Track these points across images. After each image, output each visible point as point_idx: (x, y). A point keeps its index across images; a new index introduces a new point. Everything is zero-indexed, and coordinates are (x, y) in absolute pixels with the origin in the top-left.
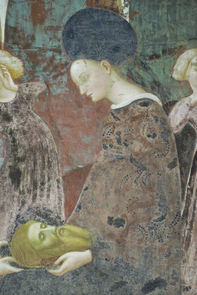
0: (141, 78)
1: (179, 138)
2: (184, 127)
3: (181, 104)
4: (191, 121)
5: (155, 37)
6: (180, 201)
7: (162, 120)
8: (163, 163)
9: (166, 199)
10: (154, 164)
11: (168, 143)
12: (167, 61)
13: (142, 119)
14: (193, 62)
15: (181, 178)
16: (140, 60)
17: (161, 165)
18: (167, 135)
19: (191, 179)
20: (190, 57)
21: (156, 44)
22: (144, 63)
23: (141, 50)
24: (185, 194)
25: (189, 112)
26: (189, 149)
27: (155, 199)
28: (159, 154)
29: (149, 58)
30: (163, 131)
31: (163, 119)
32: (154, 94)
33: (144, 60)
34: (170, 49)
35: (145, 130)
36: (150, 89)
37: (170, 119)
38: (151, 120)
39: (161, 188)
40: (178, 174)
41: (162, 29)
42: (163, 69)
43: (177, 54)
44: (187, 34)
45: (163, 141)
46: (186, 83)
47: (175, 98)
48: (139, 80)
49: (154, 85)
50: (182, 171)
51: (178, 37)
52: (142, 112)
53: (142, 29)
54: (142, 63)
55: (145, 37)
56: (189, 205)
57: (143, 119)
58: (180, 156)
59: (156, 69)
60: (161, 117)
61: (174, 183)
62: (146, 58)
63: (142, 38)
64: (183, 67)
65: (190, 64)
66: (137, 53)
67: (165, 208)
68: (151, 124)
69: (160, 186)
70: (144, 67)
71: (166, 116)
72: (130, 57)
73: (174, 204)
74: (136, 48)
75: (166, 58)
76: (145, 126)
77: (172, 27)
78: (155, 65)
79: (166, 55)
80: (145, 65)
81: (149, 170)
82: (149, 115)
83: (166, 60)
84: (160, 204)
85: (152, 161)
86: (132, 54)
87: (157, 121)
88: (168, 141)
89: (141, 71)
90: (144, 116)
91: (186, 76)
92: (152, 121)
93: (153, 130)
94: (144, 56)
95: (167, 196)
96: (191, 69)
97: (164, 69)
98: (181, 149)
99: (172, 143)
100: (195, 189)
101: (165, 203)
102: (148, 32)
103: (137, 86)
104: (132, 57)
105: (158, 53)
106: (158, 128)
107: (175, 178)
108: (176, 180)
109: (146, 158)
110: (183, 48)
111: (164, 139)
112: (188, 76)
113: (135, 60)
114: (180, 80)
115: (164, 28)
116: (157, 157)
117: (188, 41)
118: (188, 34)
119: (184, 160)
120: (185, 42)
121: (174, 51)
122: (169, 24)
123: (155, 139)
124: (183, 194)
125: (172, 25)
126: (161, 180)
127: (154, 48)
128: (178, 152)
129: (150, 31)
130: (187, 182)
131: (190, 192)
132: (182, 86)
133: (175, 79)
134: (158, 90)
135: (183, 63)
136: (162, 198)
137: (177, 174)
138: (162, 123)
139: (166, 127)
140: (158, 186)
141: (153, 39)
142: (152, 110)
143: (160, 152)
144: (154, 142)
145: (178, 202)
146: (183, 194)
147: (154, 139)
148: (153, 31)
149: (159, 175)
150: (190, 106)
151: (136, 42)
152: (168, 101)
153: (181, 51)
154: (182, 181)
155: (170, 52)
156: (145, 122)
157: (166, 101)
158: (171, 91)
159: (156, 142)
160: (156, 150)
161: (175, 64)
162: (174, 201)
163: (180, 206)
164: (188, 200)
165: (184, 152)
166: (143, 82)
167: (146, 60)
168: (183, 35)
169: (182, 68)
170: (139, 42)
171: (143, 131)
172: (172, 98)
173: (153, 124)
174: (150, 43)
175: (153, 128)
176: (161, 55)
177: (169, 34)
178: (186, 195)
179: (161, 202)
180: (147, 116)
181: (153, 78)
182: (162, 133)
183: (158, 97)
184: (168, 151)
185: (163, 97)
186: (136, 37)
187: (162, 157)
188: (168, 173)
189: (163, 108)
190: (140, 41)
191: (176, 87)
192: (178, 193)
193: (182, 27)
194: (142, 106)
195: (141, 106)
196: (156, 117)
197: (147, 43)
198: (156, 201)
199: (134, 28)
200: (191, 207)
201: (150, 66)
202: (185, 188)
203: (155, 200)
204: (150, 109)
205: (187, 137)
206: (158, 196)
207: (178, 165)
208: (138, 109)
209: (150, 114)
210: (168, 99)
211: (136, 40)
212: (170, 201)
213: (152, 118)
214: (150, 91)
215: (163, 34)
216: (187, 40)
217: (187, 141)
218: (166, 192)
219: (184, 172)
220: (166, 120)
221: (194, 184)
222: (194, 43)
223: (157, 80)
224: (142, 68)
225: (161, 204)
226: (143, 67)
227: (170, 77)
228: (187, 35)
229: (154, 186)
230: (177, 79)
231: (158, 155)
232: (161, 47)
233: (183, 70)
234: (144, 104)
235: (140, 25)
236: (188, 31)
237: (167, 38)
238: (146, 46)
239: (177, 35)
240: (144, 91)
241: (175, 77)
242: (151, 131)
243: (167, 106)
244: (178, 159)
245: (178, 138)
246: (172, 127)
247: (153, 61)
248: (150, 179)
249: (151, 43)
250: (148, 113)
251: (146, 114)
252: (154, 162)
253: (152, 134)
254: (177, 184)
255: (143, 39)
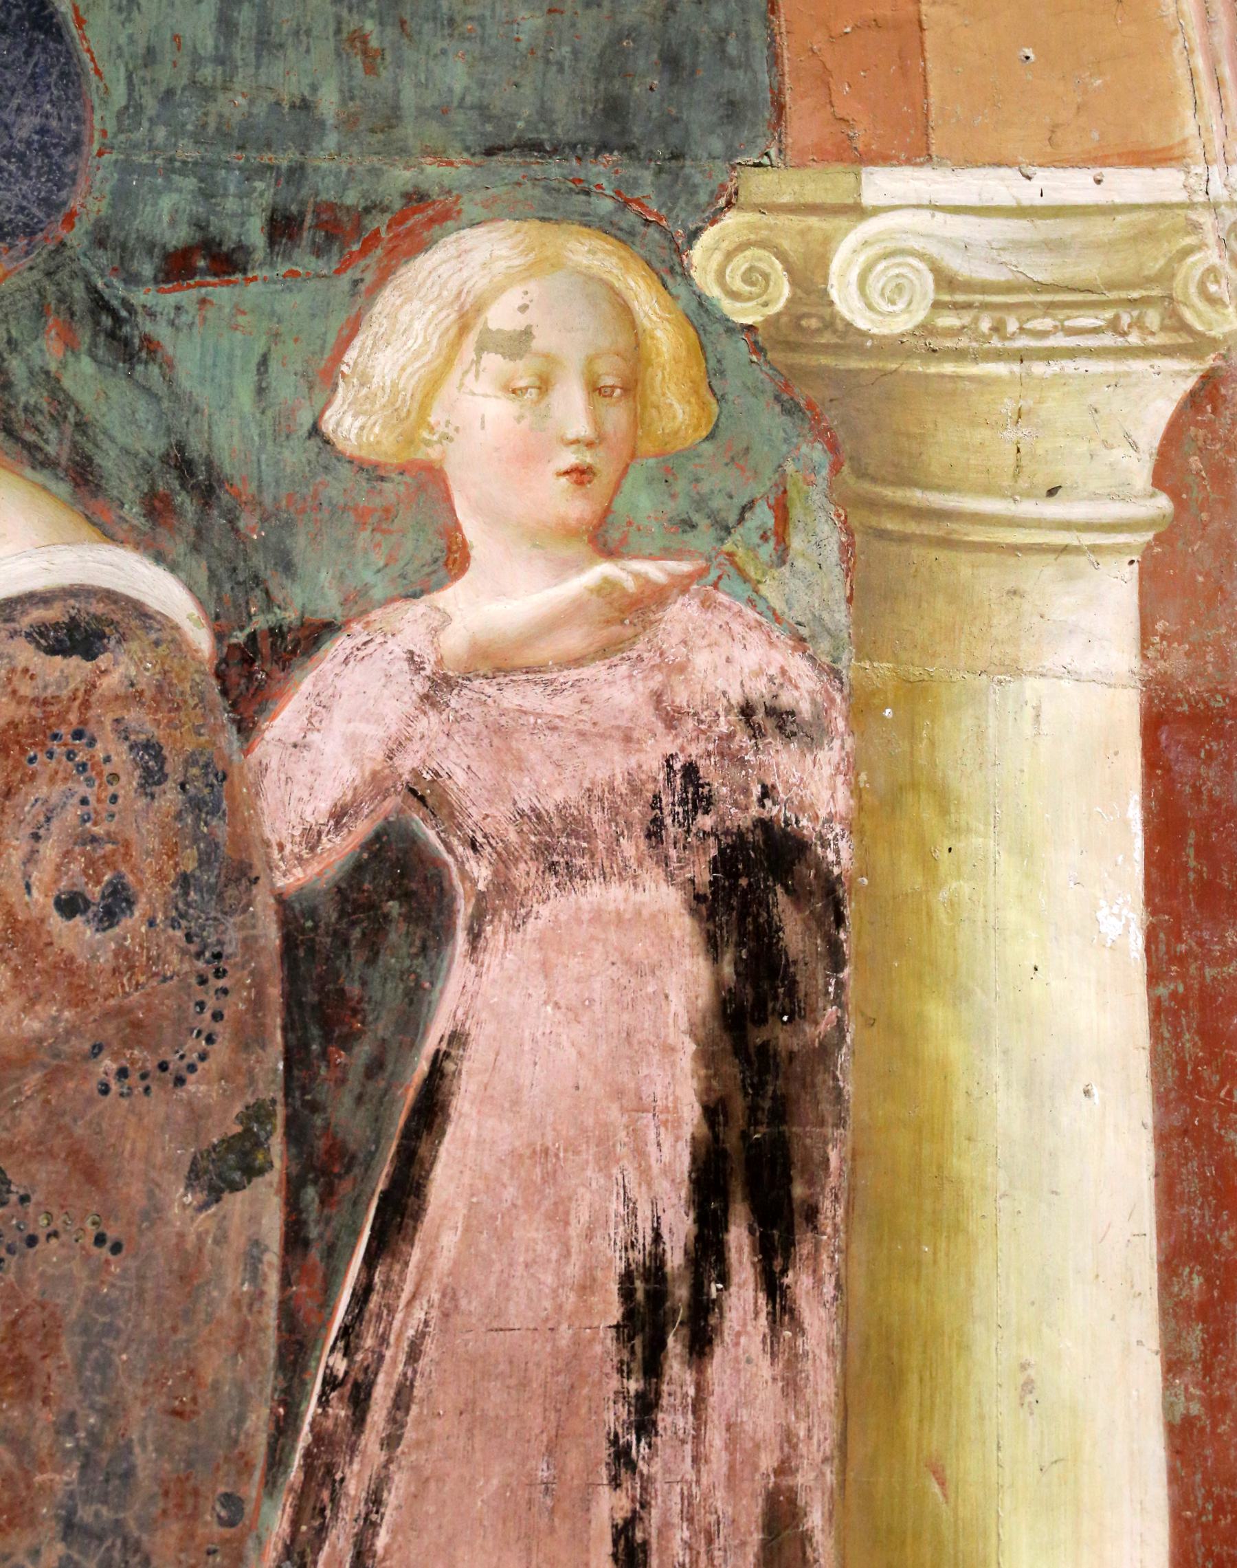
0: (77, 425)
1: (315, 928)
2: (366, 846)
3: (361, 654)
4: (422, 799)
5: (227, 111)
6: (252, 1489)
7: (195, 771)
8: (150, 1148)
9: (128, 1475)
10: (74, 1153)
11: (220, 974)
12: (294, 302)
13: (31, 760)
14: (493, 326)
15: (286, 1282)
16: (86, 277)
17: (132, 1155)
18: (221, 898)
19: (362, 1295)
20: (480, 282)
21: (228, 166)
22: (115, 303)
23: (109, 197)
24: (297, 1431)
25: (422, 725)
26: (382, 1027)
27: (42, 1467)
28: (133, 1062)
29: (158, 270)
30: (190, 866)
31: (207, 766)
32: (159, 558)
33: (116, 282)
34: (331, 207)
35: (50, 851)
36: (133, 512)
37: (263, 769)
38: (108, 769)
39: (104, 1365)
40: (266, 1249)
41: (291, 53)
42: (256, 359)
43: (379, 252)
44: (472, 108)
45: (184, 952)
46: (421, 487)
47: (323, 596)
48: (53, 435)
49: (168, 482)
50: (305, 1223)
51: (399, 118)
52: (45, 703)
53: (131, 39)
54: (99, 304)
55: (151, 105)
56: (321, 1533)
57: (42, 757)
58: (304, 1090)
59: (203, 355)
60: (189, 748)
61: (220, 1323)
62: (135, 266)
63: (126, 108)
64: (417, 355)
65: (472, 339)
66: (70, 220)
67: (117, 1555)
68: (99, 801)
69: (95, 1353)
70: (112, 335)
71: (236, 745)
72: (11, 247)
73: (194, 1516)
74: (62, 179)
75: (294, 274)
76: (48, 819)
77: (364, 40)
78: (195, 331)
79: (296, 254)
80: (118, 320)
81: (24, 1199)
82: (92, 728)
83: (288, 296)
84: (72, 1512)
85: (67, 1119)
86: (30, 231)
87: (152, 778)
88: (218, 956)
89: (87, 365)
90: (55, 737)
91: (432, 430)
92: (115, 777)
93: (114, 852)
94: (124, 247)
95: (143, 1440)
96: (477, 376)
97: (264, 362)
98: (315, 1031)
99: (252, 973)
100: (388, 1385)
101: (117, 1508)
102: (175, 64)
103: (35, 484)
104: (27, 254)
105: (234, 232)
106: (154, 843)
107: (235, 1282)
108: (245, 1301)
109: (19, 1091)
110: (430, 212)
111: (189, 937)
112: (441, 429)
113: (49, 274)
114: (382, 459)
115: (303, 48)
116: (114, 1087)
117: (477, 160)
118: (483, 110)
119: (327, 1126)
120: (450, 164)
121: (358, 228)
122: (345, 13)
123: (117, 930)
124: (284, 1427)
125: (370, 26)
126: (115, 1293)
127: (207, 194)
128: (289, 1056)
129: (197, 61)
130: (327, 1324)
131: (339, 1410)
132: (387, 510)
133: (340, 447)
134: (199, 532)
135: (418, 325)
136: (105, 1456)
137: (256, 1243)
138: (190, 800)
139: (222, 831)
140: (87, 1348)
141: (212, 122)
142: (122, 691)
143: (140, 1043)
144: (105, 959)
145: (232, 1501)
146: (284, 1427)
147: (110, 932)
148: (220, 60)
149: (105, 1252)
150: (428, 672)
151: (78, 133)
152: (261, 622)
153: (410, 232)
154: (287, 1312)
155: (330, 238)
156: (52, 780)
157: (250, 616)
158: (300, 544)
159: (125, 961)
160: (110, 1028)
161: (353, 328)
162: (196, 1493)
163: (241, 1540)
164: (322, 1485)
165: (341, 1058)
166: (90, 459)
167: (132, 279)
168: (445, 112)
169: (403, 369)
170: (97, 135)
171: (31, 858)
172: (298, 602)
173: (113, 808)
174: (180, 155)
175: (111, 838)
176: (259, 255)
177: (341, 91)
178: (305, 1437)
179: (88, 1499)
180: (78, 735)
181: (169, 431)
182: (185, 881)
183: (191, 589)
184: (210, 1040)
185: (228, 587)
186: (78, 97)
187: (154, 1088)
188: (181, 1236)
189: (219, 675)
190: (104, 133)
191: (345, 508)
192: (240, 1419)
193: (444, 52)
194: (51, 651)
195: (38, 646)
196: (147, 746)
197: (153, 148)
198: (42, 1487)
199: (72, 25)
200: (333, 1547)
201: (162, 332)
202: (305, 1369)
203: (39, 1478)
204: (111, 682)
205: (381, 923)
206: (69, 1445)
207: (278, 1164)
208: (13, 670)
209: (108, 721)
210: (269, 602)
211: (78, 120)
212: (166, 1494)
213: (121, 756)
214: (133, 528)
215: (292, 88)
216: (467, 149)
217: (371, 961)
218: (144, 1402)
219: (313, 1232)
220: (225, 777)
221: (383, 1340)
222: (518, 174)
223: (196, 447)
224: (94, 344)
225: (85, 1514)
226: (102, 339)
227: (307, 425)
228: (474, 115)
229: (51, 1351)
230: (360, 446)
231: (123, 1073)
232: (265, 192)
233: (413, 382)
234: (71, 637)
235: (120, 10)
236: (482, 85)
237: (321, 124)
238: (145, 170)
239: (396, 108)
240: (86, 530)
241: (342, 432)
242: (91, 863)
243: (252, 662)
244: (281, 1111)
245: (303, 930)
246: (268, 834)
247: (187, 296)
248: (21, 1280)
249: (188, 151)
250: (91, 713)
251: (73, 717)
252: (79, 1130)
253: (95, 892)
254: (243, 1338)
255: (131, 112)
